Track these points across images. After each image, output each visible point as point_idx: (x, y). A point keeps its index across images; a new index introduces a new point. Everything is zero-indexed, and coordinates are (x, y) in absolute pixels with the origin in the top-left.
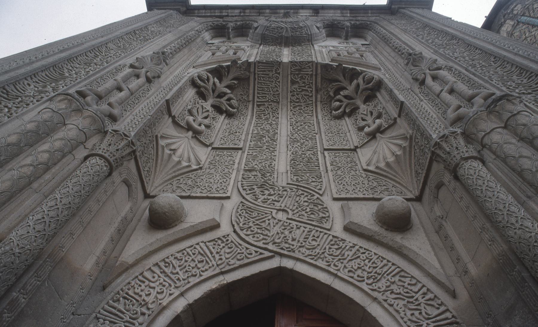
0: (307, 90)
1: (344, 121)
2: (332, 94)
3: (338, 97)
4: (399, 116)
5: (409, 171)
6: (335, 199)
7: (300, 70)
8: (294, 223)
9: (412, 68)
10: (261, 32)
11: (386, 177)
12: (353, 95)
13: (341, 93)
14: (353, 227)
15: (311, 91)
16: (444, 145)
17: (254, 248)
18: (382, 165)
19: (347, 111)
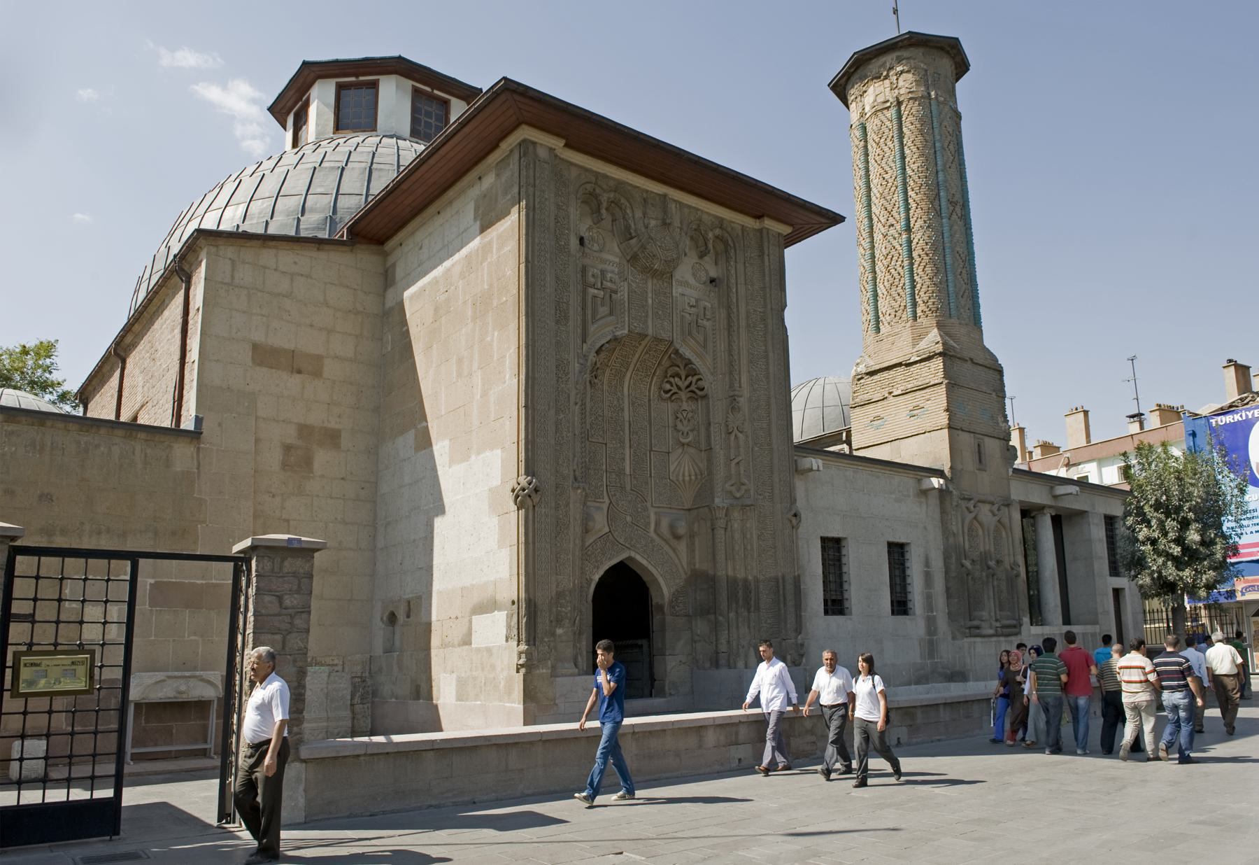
2: (668, 376)
3: (672, 379)
4: (705, 450)
7: (657, 345)
8: (636, 527)
10: (635, 249)
13: (676, 379)
16: (717, 512)
17: (620, 545)
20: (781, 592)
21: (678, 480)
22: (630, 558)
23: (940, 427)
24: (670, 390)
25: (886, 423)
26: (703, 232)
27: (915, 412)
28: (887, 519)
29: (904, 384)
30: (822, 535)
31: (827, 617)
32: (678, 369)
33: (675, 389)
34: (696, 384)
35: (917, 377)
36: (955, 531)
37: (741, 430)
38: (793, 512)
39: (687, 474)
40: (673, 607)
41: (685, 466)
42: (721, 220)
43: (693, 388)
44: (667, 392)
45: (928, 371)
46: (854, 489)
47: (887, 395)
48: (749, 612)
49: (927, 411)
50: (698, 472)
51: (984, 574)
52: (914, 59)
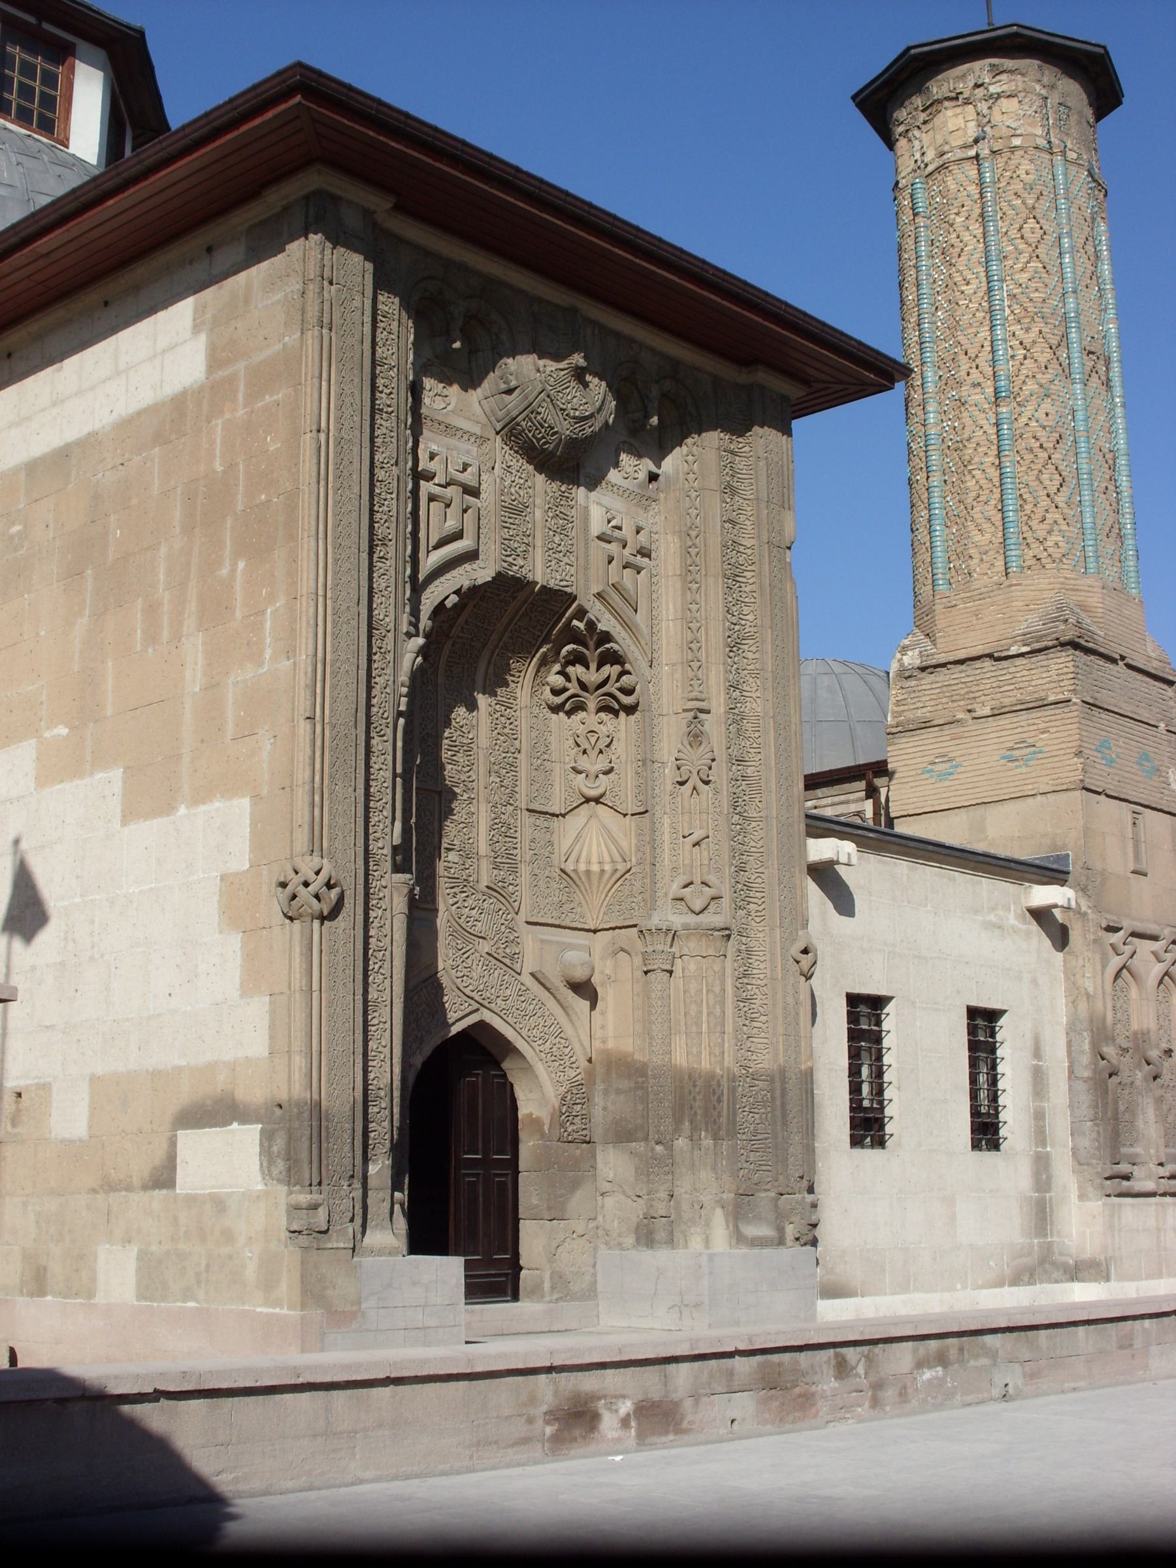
0: (534, 634)
1: (554, 716)
5: (604, 895)
6: (528, 923)
7: (546, 601)
9: (686, 743)
11: (577, 886)
12: (591, 688)
14: (539, 976)
15: (539, 636)
18: (582, 867)
19: (567, 707)
20: (778, 1103)
21: (575, 871)
22: (482, 1025)
23: (1065, 787)
24: (565, 690)
25: (960, 769)
26: (640, 384)
27: (1016, 753)
28: (967, 963)
29: (995, 696)
30: (850, 991)
31: (858, 1152)
32: (584, 650)
33: (573, 688)
34: (617, 681)
35: (1022, 685)
36: (1091, 990)
37: (705, 778)
38: (801, 945)
39: (594, 859)
40: (562, 1125)
41: (590, 845)
42: (676, 363)
43: (610, 688)
44: (556, 692)
45: (1044, 675)
46: (909, 902)
47: (960, 716)
48: (716, 1138)
49: (1040, 752)
50: (617, 857)
51: (1139, 1075)
52: (1023, 75)
